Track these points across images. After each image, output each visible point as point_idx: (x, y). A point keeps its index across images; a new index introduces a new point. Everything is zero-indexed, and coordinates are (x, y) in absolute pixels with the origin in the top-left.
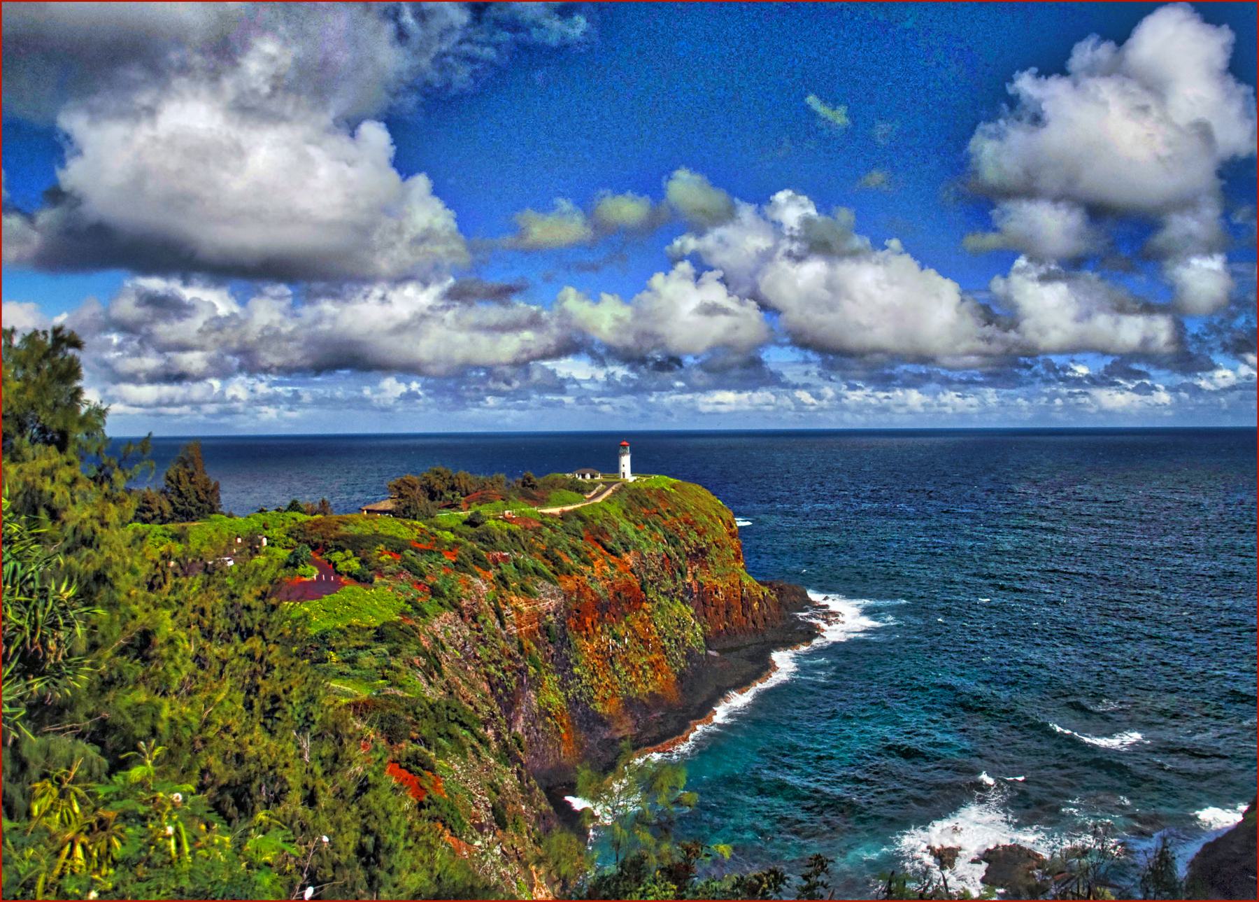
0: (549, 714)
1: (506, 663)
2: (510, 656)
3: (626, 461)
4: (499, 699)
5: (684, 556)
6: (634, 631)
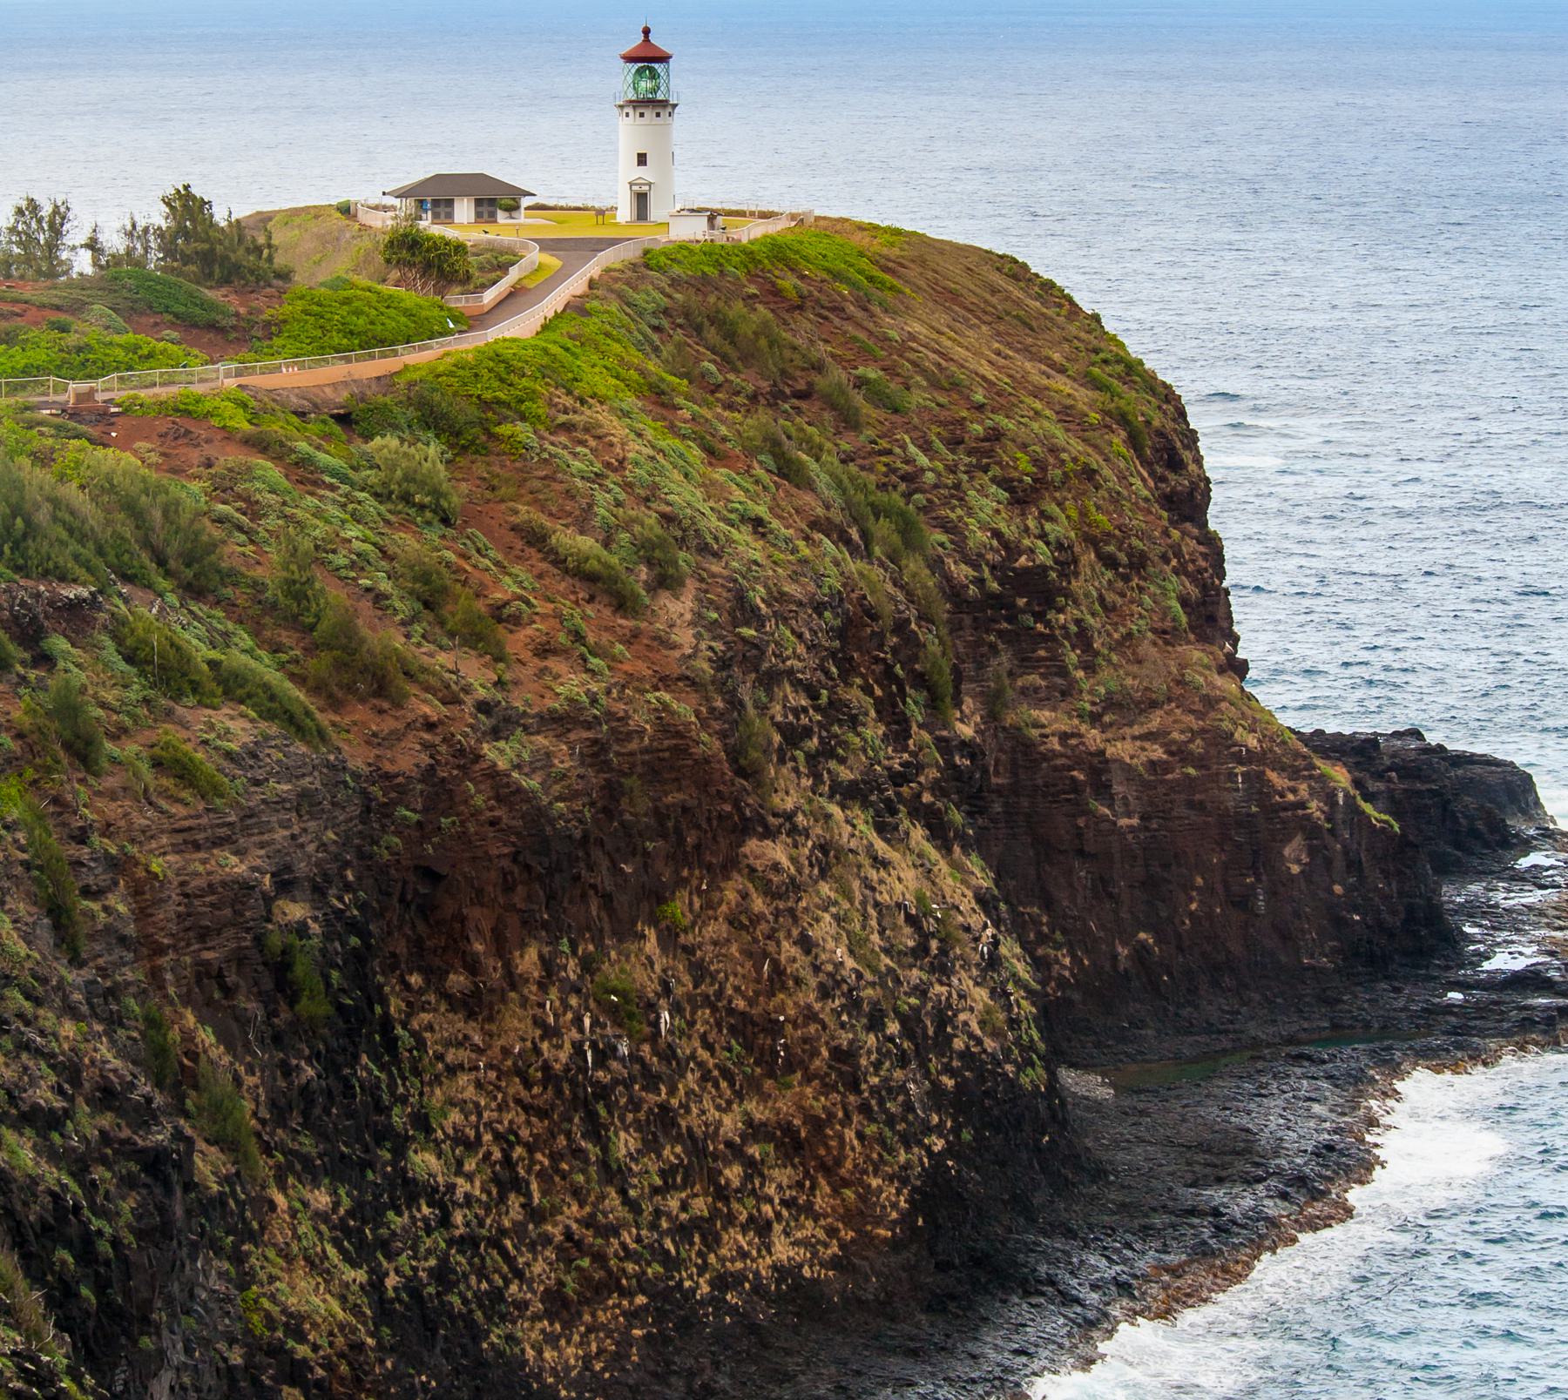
1: (89, 1123)
2: (108, 1096)
4: (61, 1299)
5: (943, 609)
6: (700, 972)
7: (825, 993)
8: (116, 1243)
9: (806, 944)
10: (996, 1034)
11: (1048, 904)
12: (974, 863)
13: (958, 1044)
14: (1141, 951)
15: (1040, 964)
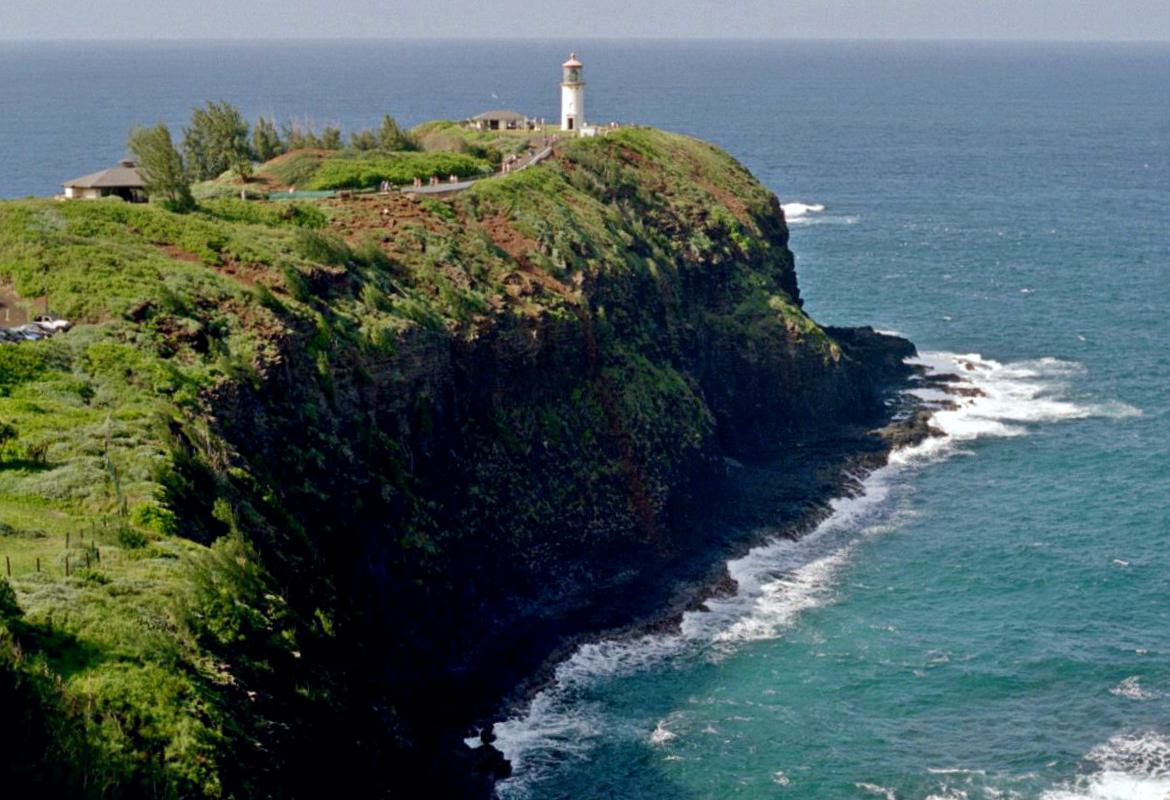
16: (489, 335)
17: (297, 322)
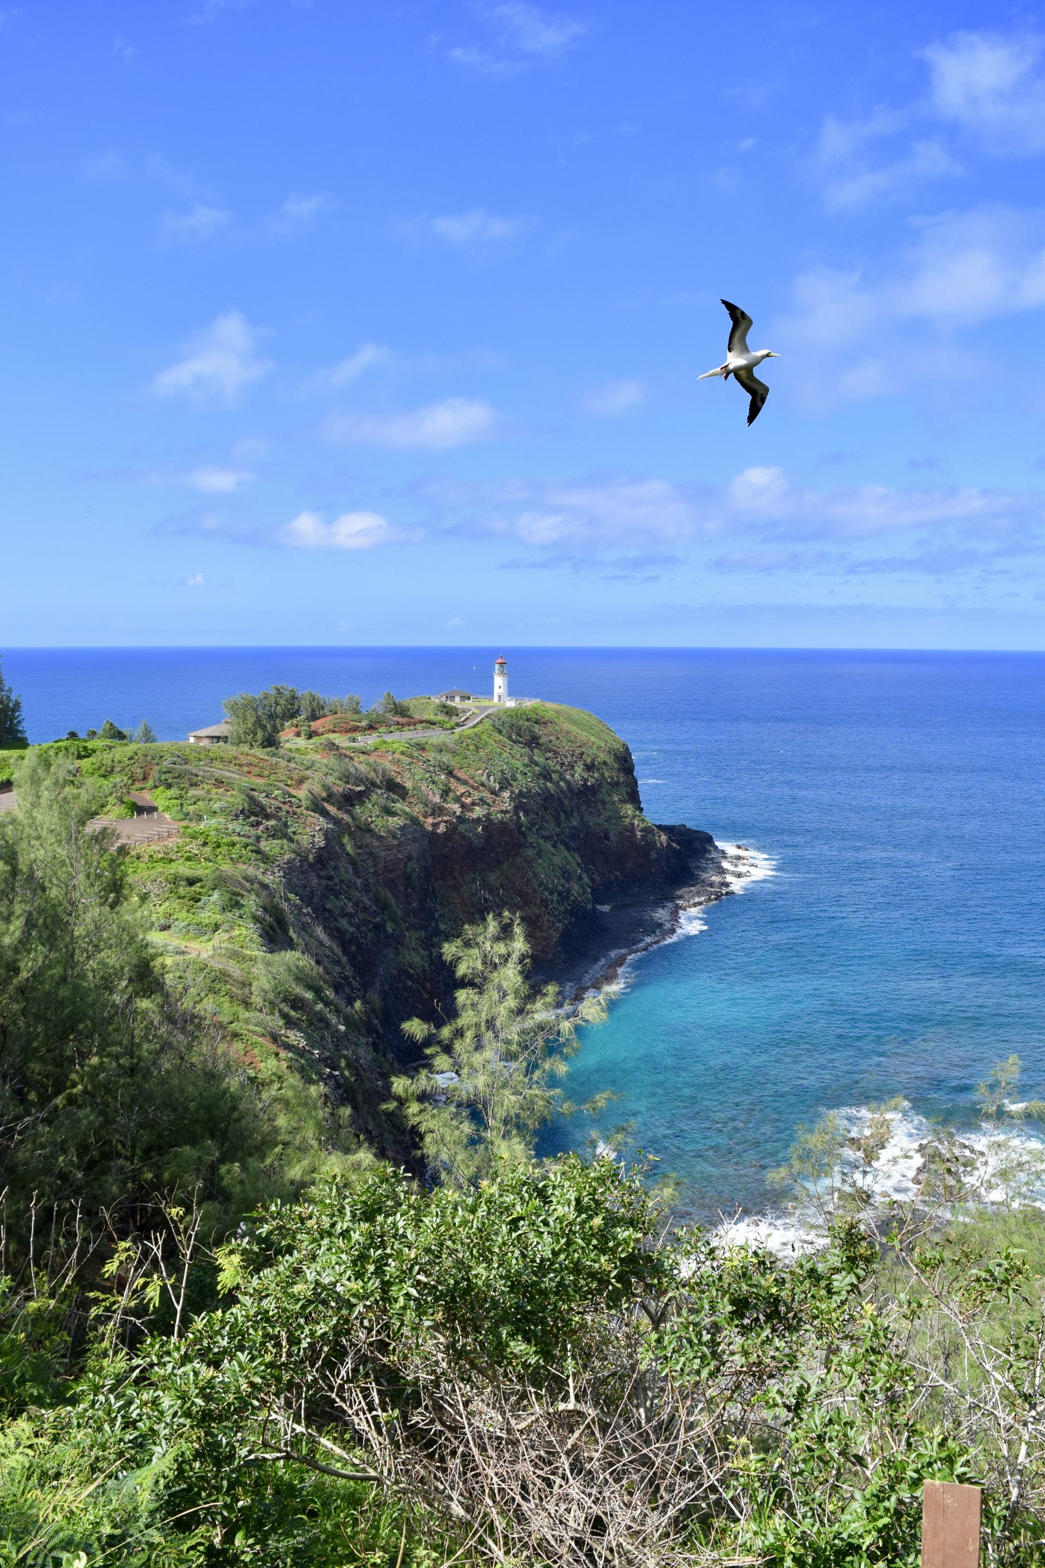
0: (410, 976)
2: (365, 909)
3: (499, 682)
4: (352, 960)
7: (540, 886)
8: (367, 945)
9: (535, 874)
10: (580, 896)
11: (594, 865)
12: (576, 855)
13: (572, 898)
14: (617, 877)
15: (592, 880)
16: (452, 829)
17: (336, 821)
